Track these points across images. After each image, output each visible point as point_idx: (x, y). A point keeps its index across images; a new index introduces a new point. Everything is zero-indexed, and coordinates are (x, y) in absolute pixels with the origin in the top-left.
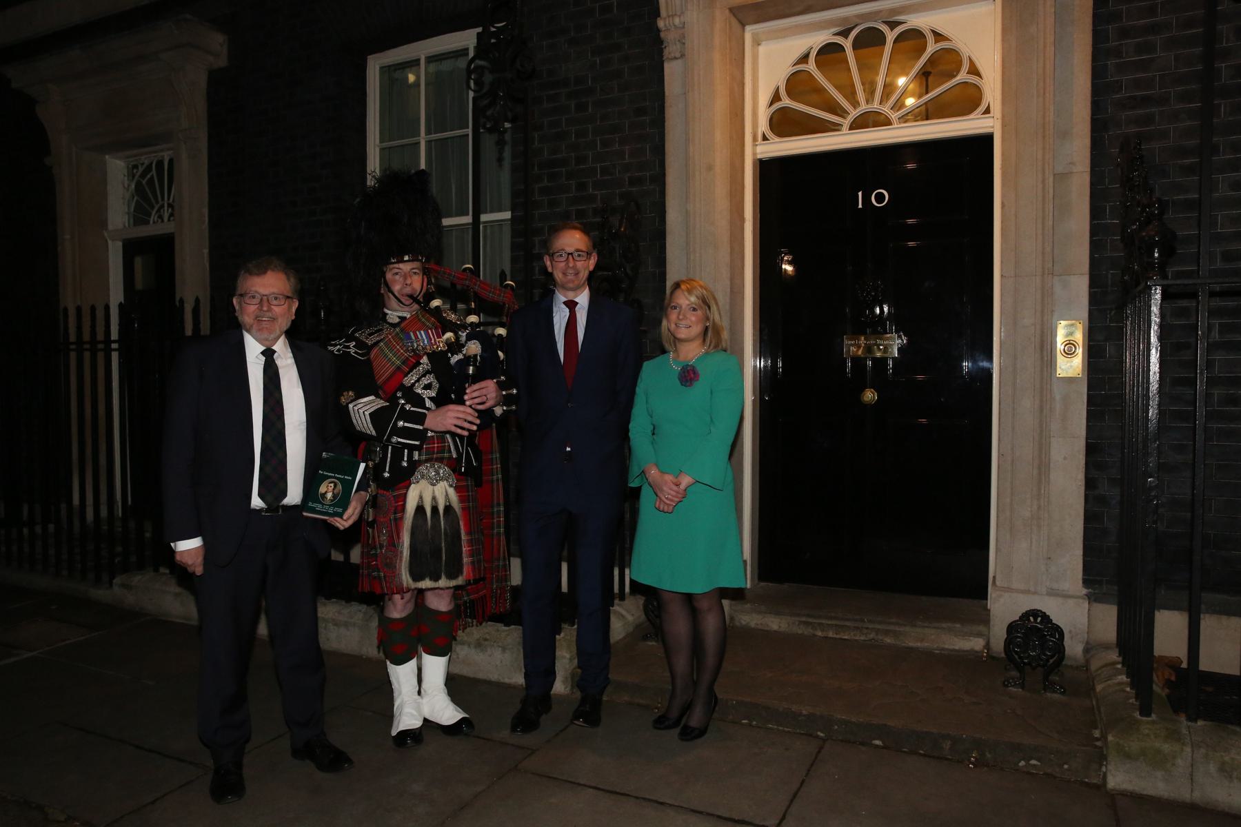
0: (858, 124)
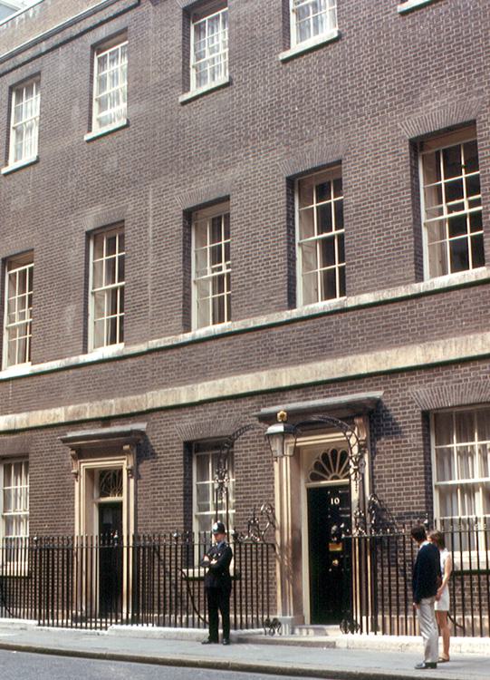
0: (332, 479)
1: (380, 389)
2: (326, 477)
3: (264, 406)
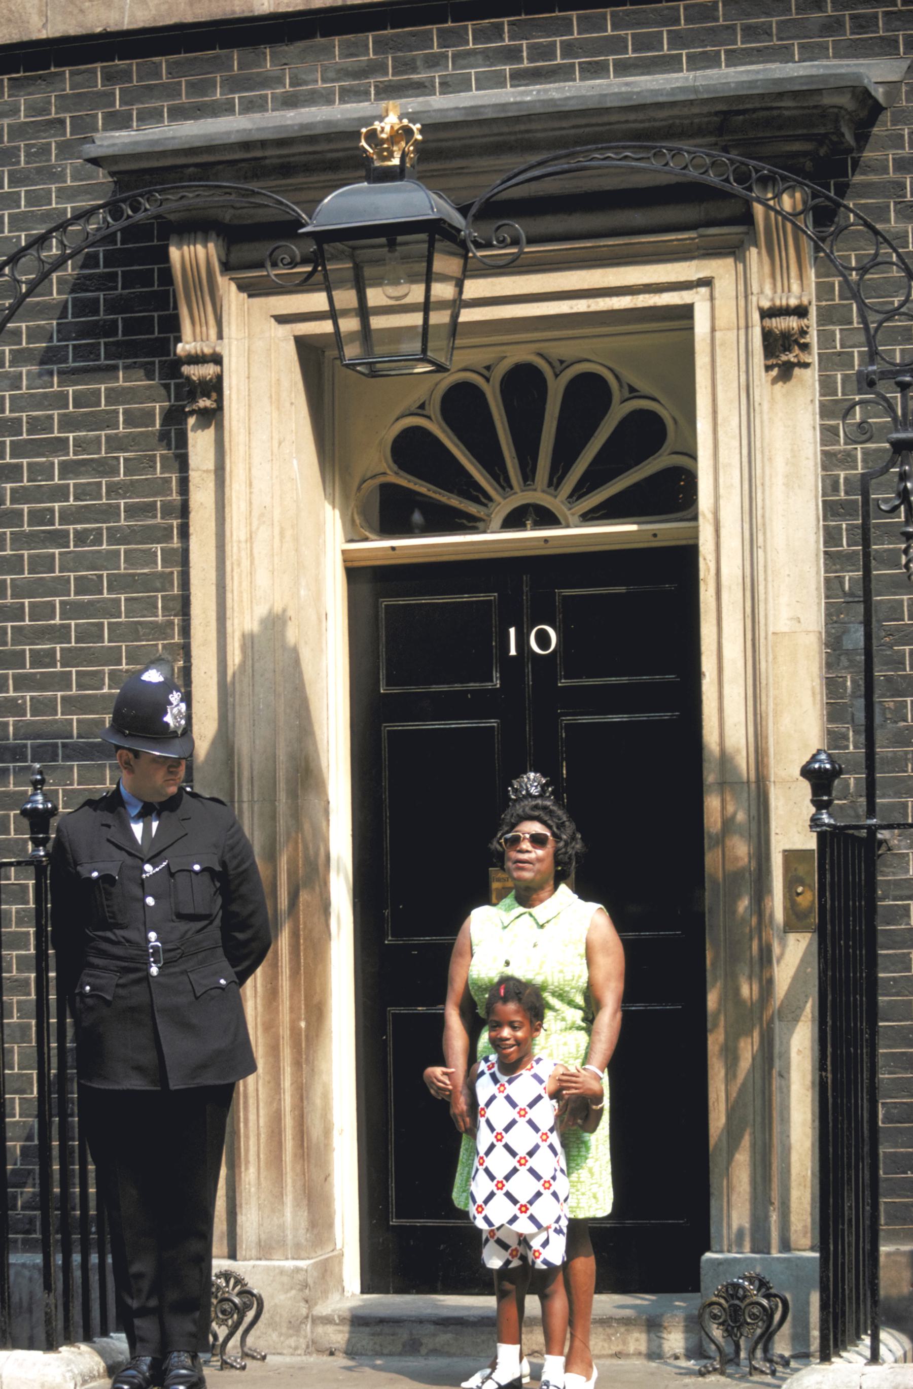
1: (888, 47)
2: (472, 509)
3: (118, 121)
